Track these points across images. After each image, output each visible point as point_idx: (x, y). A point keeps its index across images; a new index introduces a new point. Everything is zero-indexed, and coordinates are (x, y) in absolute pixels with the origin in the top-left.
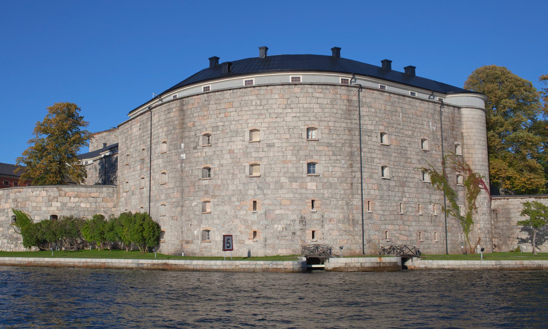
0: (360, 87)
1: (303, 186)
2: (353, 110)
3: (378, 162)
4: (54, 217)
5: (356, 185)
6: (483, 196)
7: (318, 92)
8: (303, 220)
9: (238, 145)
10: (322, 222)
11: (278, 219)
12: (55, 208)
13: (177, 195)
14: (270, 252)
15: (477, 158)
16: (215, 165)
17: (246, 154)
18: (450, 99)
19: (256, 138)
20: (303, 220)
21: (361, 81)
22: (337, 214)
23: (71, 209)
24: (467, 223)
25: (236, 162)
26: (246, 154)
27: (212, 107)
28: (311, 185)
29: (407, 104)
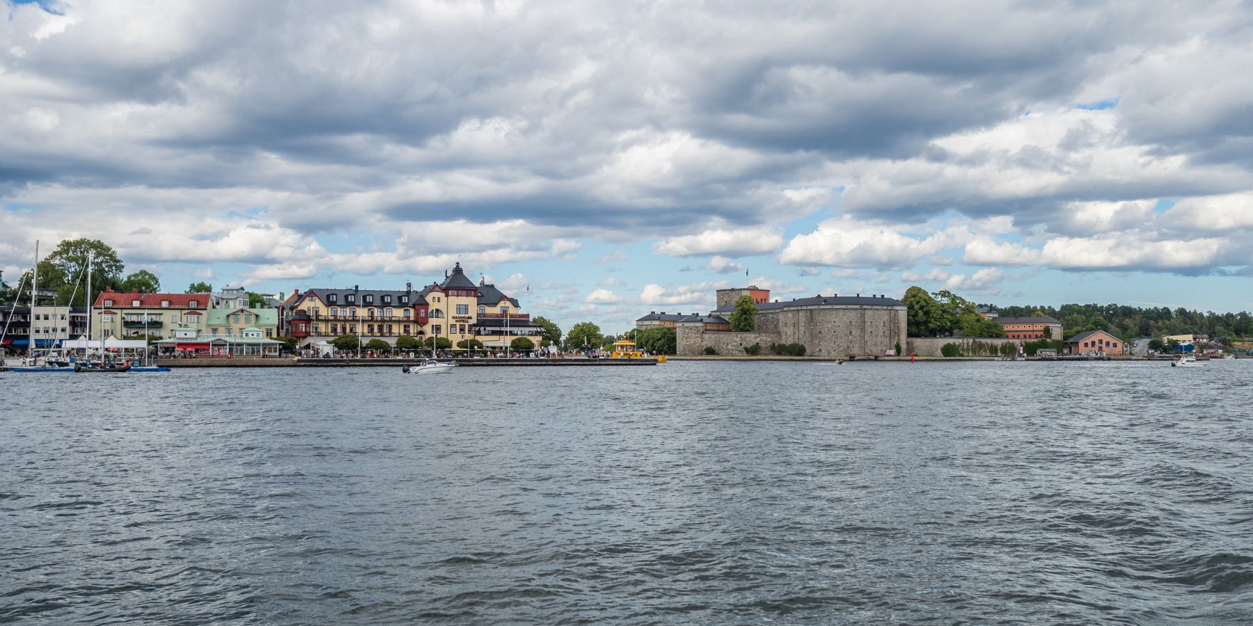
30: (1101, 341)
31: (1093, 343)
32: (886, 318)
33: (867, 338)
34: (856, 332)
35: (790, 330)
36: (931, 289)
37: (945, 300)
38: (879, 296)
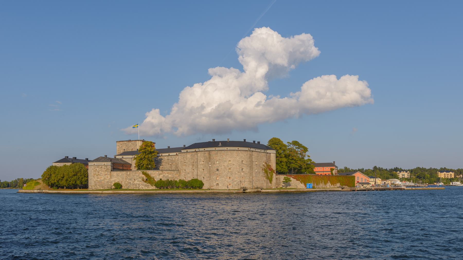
0: (252, 151)
1: (241, 174)
2: (251, 156)
4: (161, 179)
5: (251, 174)
6: (274, 175)
7: (244, 153)
8: (241, 181)
10: (245, 182)
11: (235, 181)
12: (161, 177)
13: (208, 175)
14: (233, 188)
15: (274, 166)
16: (220, 168)
17: (228, 166)
18: (269, 151)
19: (230, 163)
20: (241, 181)
21: (252, 149)
22: (247, 180)
23: (166, 177)
24: (271, 181)
26: (228, 166)
27: (219, 154)
28: (242, 174)
32: (265, 159)
33: (254, 175)
34: (246, 170)
35: (189, 169)
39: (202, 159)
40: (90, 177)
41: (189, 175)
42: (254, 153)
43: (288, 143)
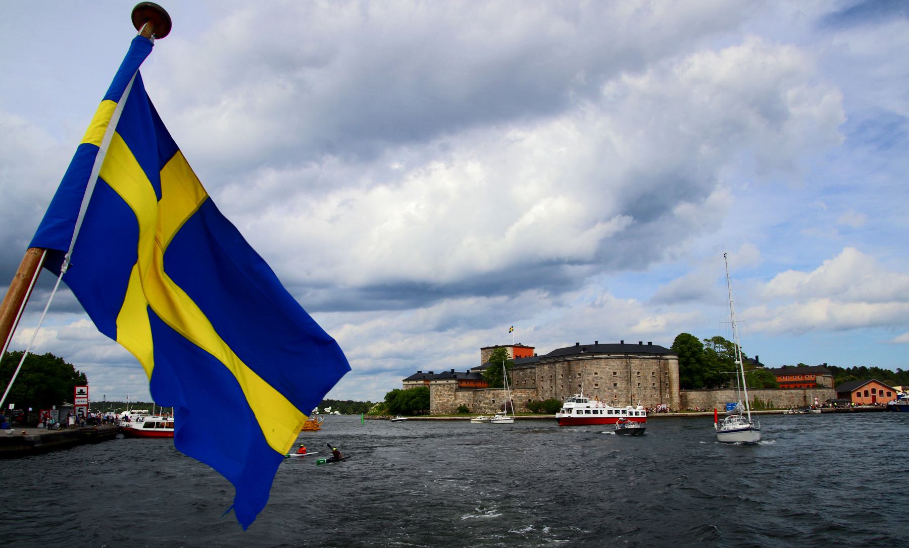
0: (630, 358)
3: (637, 382)
7: (616, 361)
9: (590, 378)
22: (624, 400)
25: (590, 383)
27: (581, 364)
29: (647, 361)
30: (874, 391)
31: (866, 393)
32: (655, 367)
33: (634, 391)
34: (621, 385)
35: (546, 385)
36: (702, 335)
37: (719, 349)
38: (645, 343)
39: (561, 373)
40: (432, 399)
41: (547, 394)
42: (633, 361)
43: (706, 340)
